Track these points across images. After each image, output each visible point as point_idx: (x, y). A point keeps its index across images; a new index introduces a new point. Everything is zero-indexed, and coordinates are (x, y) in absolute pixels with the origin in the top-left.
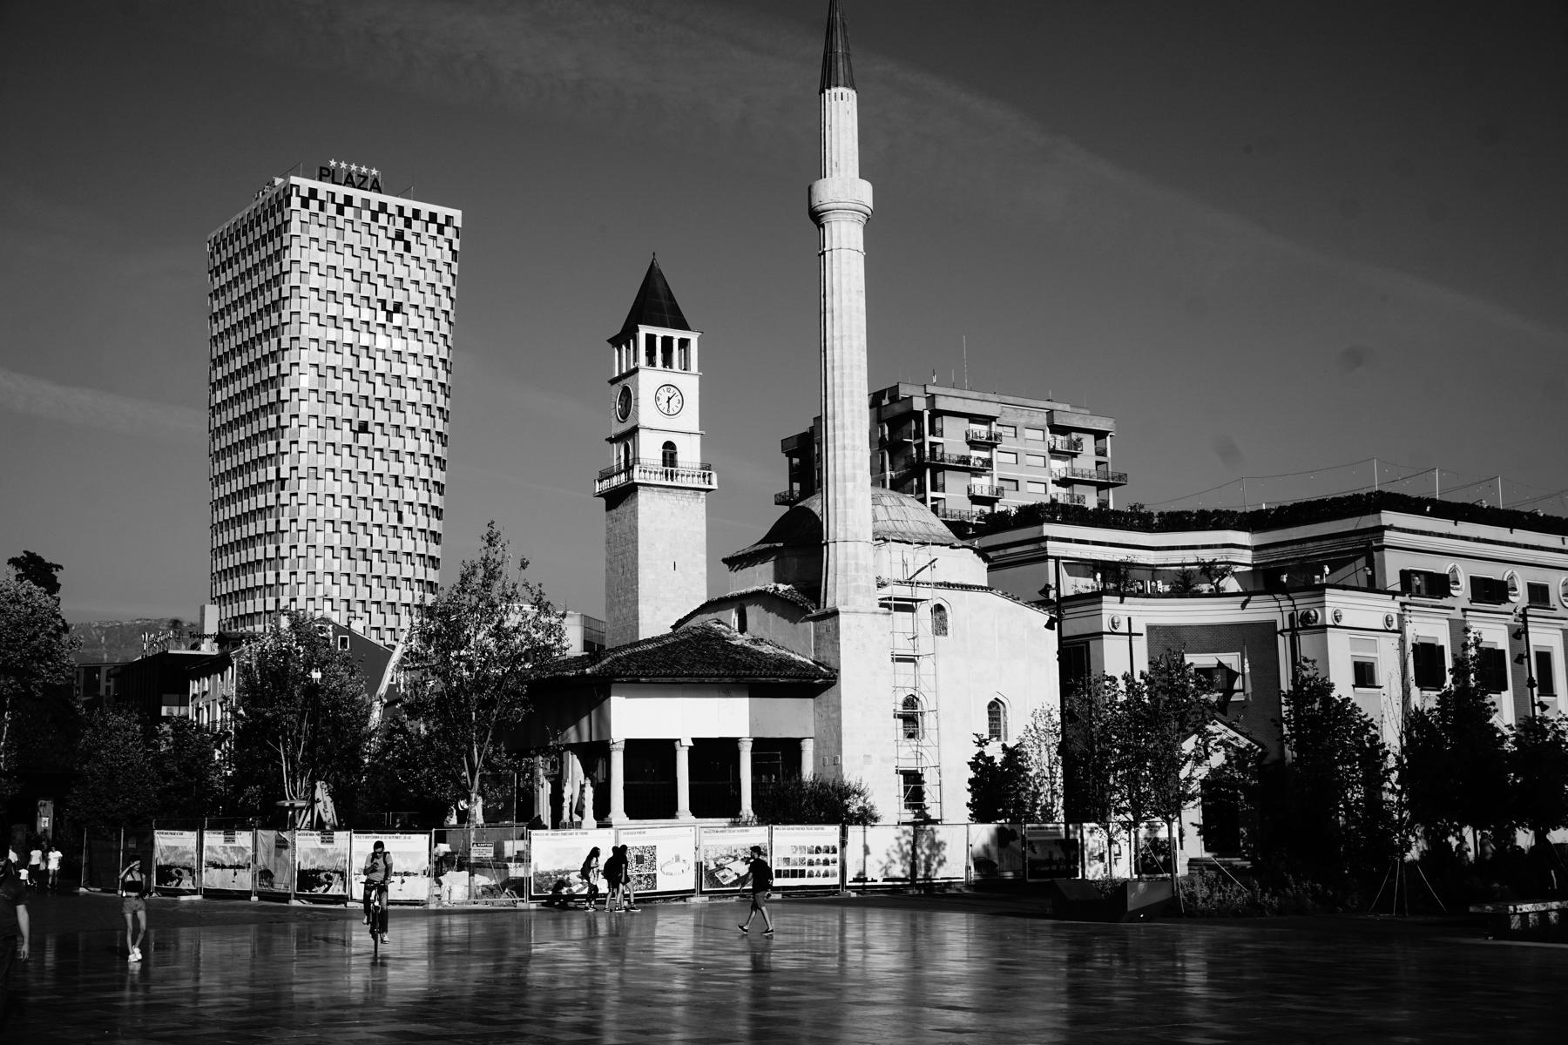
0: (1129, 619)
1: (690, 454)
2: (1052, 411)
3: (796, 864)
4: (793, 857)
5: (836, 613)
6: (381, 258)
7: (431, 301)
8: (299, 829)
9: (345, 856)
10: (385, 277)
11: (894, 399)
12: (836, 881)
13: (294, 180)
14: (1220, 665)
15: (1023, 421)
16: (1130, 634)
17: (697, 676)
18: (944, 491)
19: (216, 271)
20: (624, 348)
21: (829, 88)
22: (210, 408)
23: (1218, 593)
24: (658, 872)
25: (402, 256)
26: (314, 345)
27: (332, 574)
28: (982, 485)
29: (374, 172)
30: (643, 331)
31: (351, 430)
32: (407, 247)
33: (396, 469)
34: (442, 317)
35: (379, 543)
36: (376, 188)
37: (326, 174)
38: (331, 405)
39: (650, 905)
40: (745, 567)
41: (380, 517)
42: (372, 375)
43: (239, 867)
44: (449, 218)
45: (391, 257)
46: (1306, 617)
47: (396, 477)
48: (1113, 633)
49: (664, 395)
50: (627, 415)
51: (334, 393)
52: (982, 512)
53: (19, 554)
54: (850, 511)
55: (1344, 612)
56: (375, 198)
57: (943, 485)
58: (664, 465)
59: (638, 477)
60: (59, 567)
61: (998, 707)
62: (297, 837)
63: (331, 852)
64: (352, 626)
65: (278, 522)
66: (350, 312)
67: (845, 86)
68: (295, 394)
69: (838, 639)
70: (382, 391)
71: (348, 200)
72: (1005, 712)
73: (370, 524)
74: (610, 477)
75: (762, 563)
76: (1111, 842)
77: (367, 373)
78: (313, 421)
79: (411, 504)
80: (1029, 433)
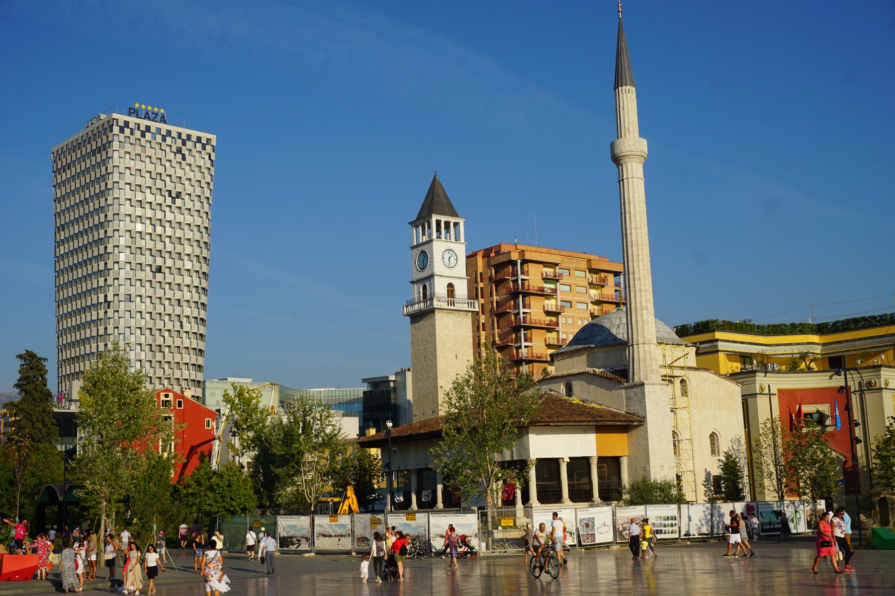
0: (769, 386)
1: (462, 290)
2: (590, 260)
3: (658, 527)
4: (658, 522)
5: (642, 384)
6: (168, 164)
7: (198, 191)
8: (340, 514)
9: (425, 527)
10: (170, 176)
11: (498, 253)
12: (676, 536)
13: (115, 116)
14: (818, 412)
15: (573, 266)
16: (770, 394)
17: (546, 422)
18: (530, 308)
19: (57, 172)
20: (420, 228)
21: (622, 86)
22: (56, 257)
23: (809, 370)
24: (596, 532)
25: (180, 163)
26: (128, 218)
27: (141, 361)
28: (551, 304)
29: (162, 111)
30: (434, 218)
31: (151, 271)
32: (184, 158)
33: (178, 295)
34: (205, 201)
35: (169, 341)
36: (163, 120)
37: (133, 112)
38: (139, 256)
39: (591, 551)
40: (566, 359)
41: (169, 326)
42: (163, 237)
43: (341, 536)
44: (208, 140)
45: (174, 164)
46: (869, 384)
47: (179, 300)
48: (761, 394)
49: (447, 256)
50: (424, 268)
51: (141, 248)
52: (551, 321)
53: (23, 352)
54: (645, 327)
55: (889, 380)
56: (164, 127)
57: (529, 305)
58: (448, 297)
59: (436, 304)
60: (45, 359)
61: (714, 437)
62: (389, 518)
63: (414, 525)
64: (185, 394)
65: (106, 329)
66: (150, 198)
67: (632, 85)
68: (116, 249)
69: (645, 399)
70: (170, 247)
71: (148, 129)
72: (718, 440)
73: (163, 330)
74: (413, 304)
75: (578, 356)
76: (796, 511)
77: (160, 236)
78: (128, 266)
79: (188, 317)
80: (577, 273)
